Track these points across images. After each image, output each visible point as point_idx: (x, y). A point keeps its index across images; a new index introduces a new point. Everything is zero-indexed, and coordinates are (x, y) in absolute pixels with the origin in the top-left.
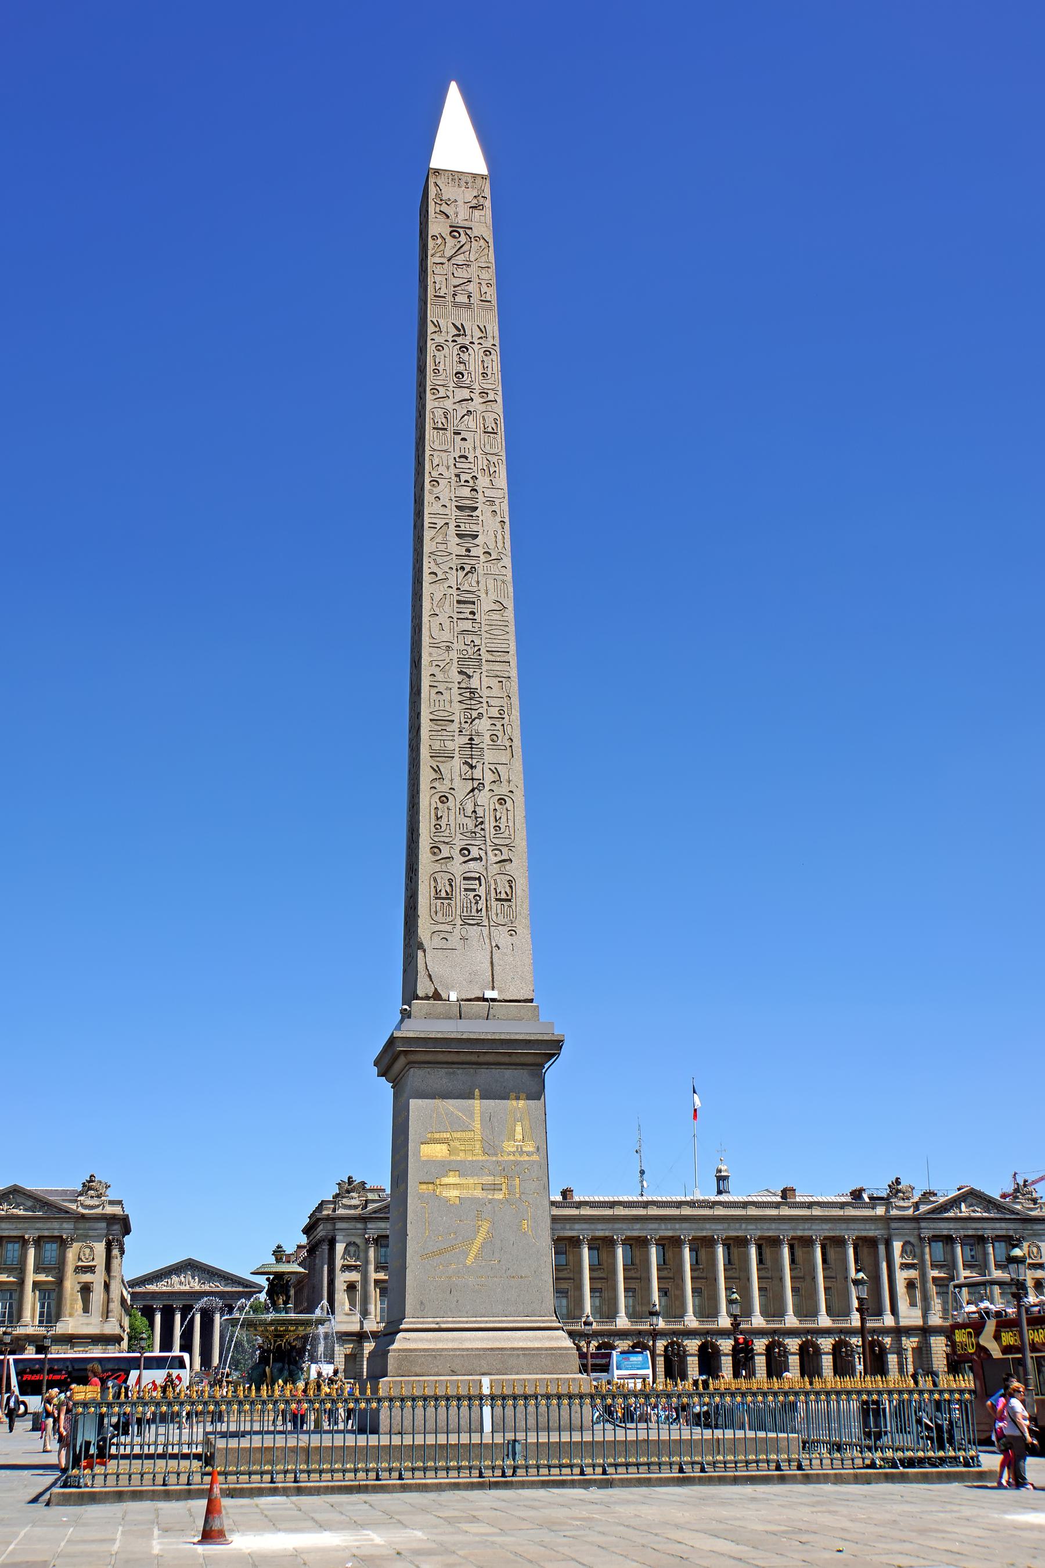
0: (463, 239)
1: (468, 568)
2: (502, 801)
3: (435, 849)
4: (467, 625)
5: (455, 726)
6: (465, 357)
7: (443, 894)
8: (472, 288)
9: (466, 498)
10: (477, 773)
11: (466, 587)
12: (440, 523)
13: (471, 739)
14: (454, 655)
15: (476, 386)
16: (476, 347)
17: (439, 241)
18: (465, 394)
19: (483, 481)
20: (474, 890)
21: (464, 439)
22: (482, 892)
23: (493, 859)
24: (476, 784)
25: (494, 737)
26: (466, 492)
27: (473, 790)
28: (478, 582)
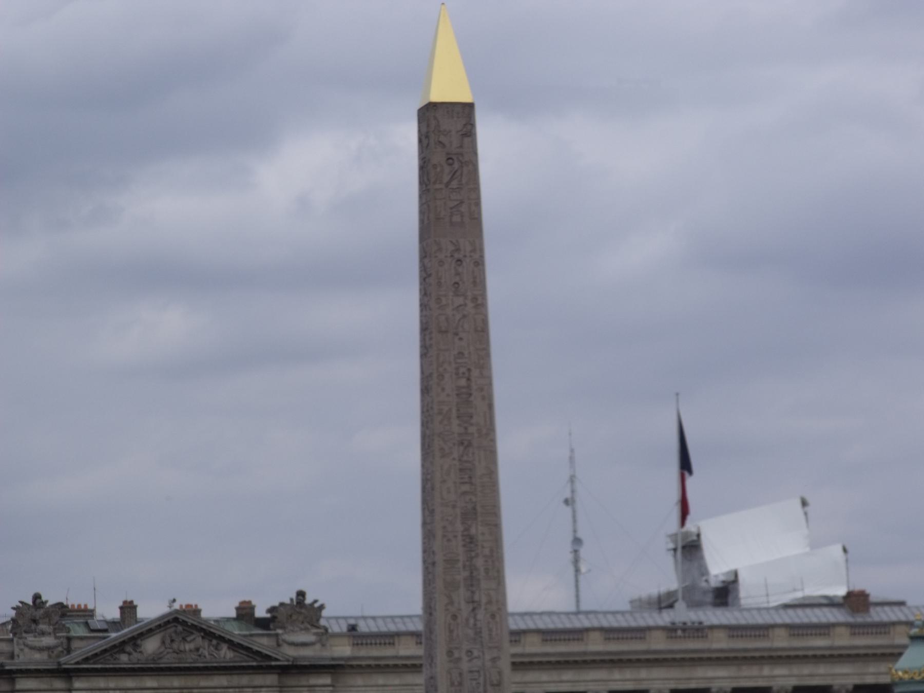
0: (456, 166)
1: (466, 443)
2: (493, 616)
3: (450, 653)
4: (466, 488)
5: (460, 565)
6: (460, 269)
7: (456, 683)
8: (464, 208)
9: (463, 387)
10: (476, 598)
11: (465, 458)
12: (446, 408)
13: (472, 573)
14: (458, 511)
15: (469, 294)
16: (468, 260)
17: (438, 169)
18: (460, 301)
19: (475, 373)
20: (475, 679)
21: (461, 339)
22: (481, 680)
23: (488, 657)
24: (475, 605)
25: (487, 571)
26: (463, 382)
27: (474, 609)
28: (473, 454)
